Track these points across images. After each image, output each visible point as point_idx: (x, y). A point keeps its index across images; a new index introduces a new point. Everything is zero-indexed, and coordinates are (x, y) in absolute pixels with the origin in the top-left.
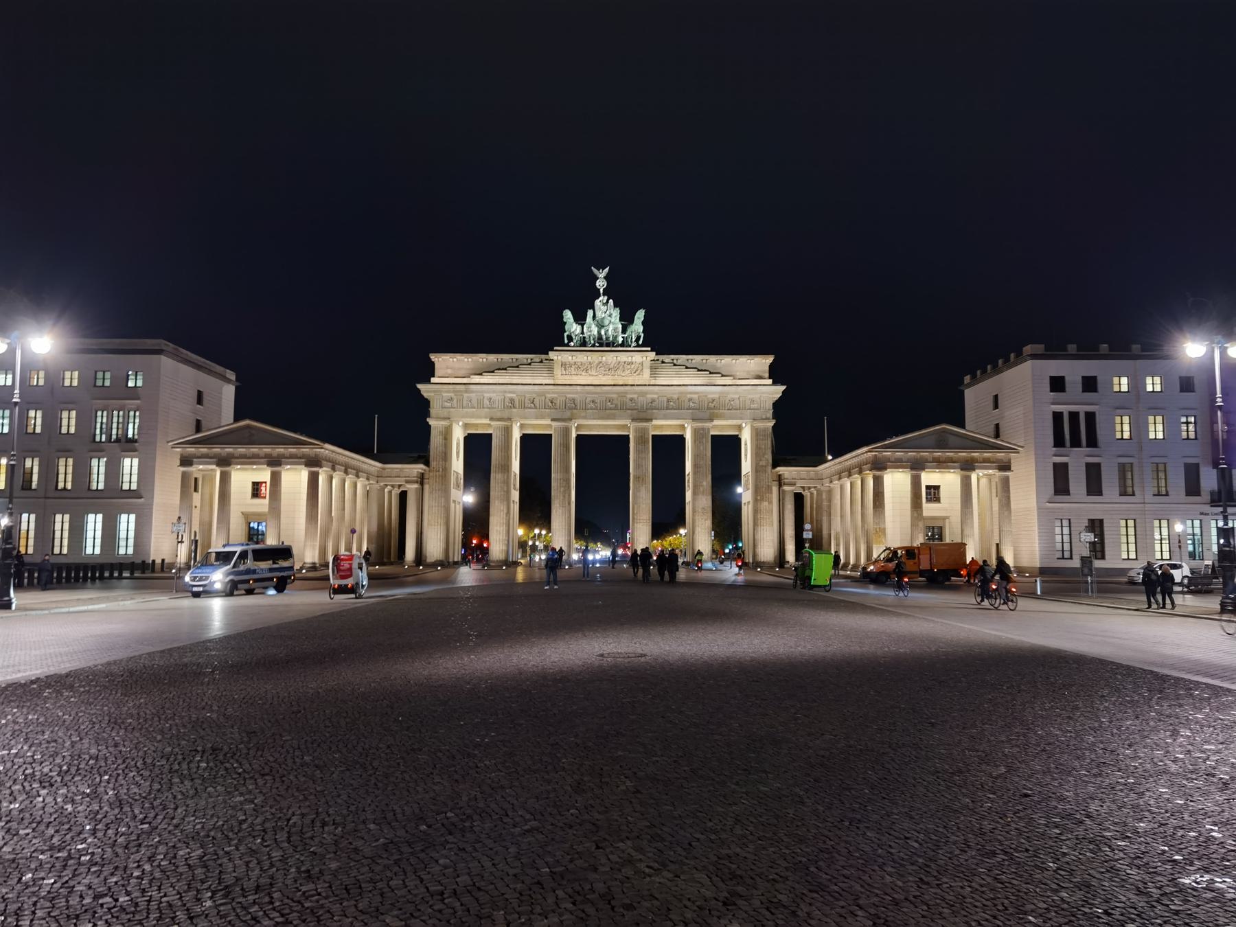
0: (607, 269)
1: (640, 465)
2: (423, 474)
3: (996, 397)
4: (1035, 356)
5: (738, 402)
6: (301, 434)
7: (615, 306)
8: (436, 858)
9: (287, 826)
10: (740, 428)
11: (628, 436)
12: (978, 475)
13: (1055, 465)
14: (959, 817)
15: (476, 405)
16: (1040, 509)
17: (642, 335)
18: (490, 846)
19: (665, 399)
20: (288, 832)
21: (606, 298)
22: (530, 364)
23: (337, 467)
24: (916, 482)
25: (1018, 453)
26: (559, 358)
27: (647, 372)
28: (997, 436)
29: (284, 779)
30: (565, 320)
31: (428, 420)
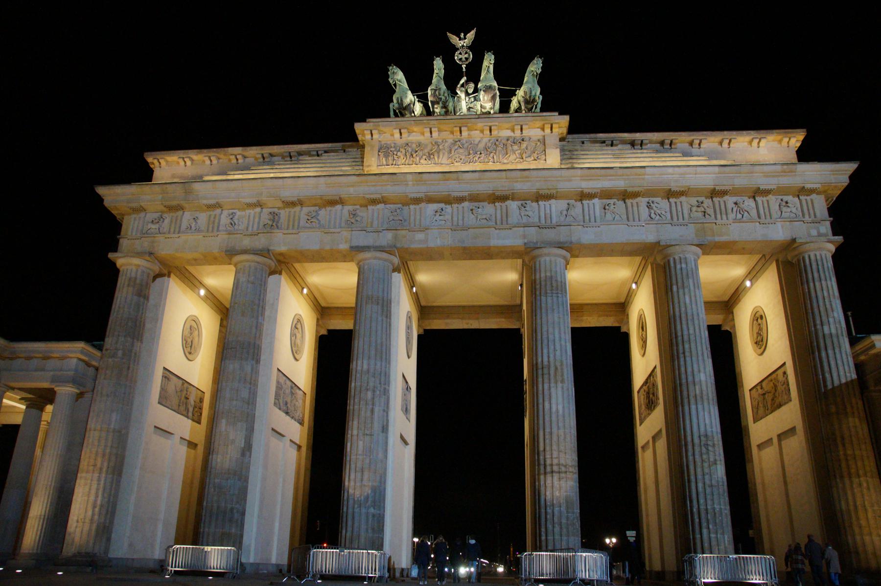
0: (473, 33)
5: (753, 204)
11: (519, 330)
26: (375, 136)
31: (111, 256)
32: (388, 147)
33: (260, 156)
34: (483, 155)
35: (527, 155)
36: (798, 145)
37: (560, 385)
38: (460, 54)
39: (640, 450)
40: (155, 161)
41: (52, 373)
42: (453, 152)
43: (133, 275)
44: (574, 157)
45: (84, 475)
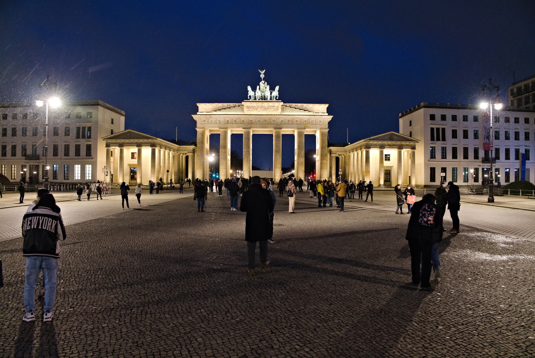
0: (265, 70)
1: (277, 145)
2: (194, 149)
3: (411, 122)
4: (424, 107)
6: (148, 135)
7: (268, 84)
8: (196, 337)
9: (130, 313)
10: (315, 132)
14: (429, 307)
16: (425, 163)
17: (278, 96)
18: (221, 331)
20: (131, 317)
21: (264, 81)
22: (234, 107)
23: (162, 147)
24: (381, 153)
27: (280, 110)
28: (411, 136)
29: (132, 286)
31: (196, 128)
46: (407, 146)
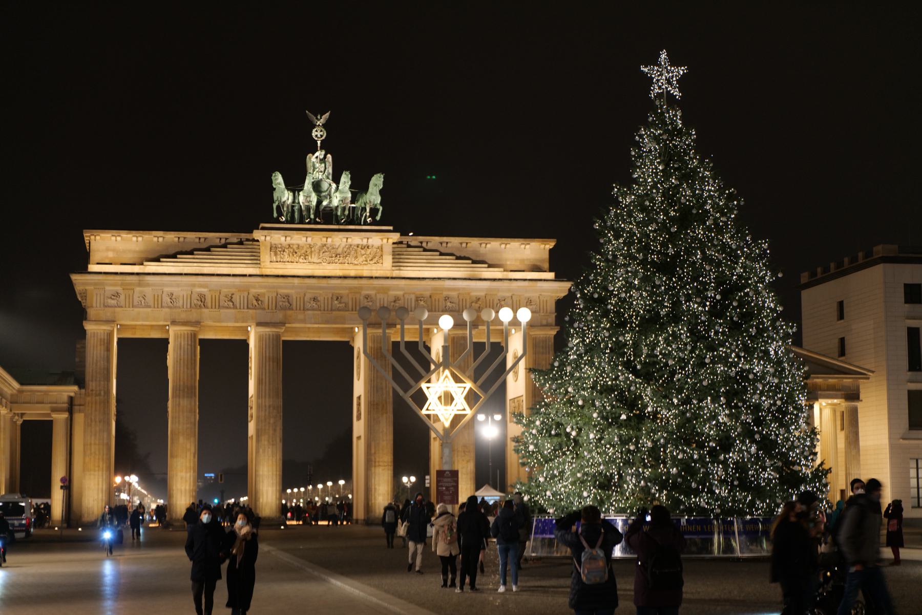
0: (327, 114)
2: (71, 399)
3: (841, 304)
4: (886, 260)
5: (511, 302)
12: (821, 404)
13: (910, 393)
15: (151, 304)
16: (893, 447)
17: (381, 208)
19: (413, 297)
21: (323, 152)
22: (225, 246)
25: (868, 378)
26: (268, 238)
27: (388, 260)
28: (842, 353)
30: (274, 187)
32: (276, 248)
33: (177, 239)
34: (341, 258)
35: (370, 259)
36: (551, 247)
37: (385, 415)
38: (317, 131)
39: (432, 440)
40: (92, 237)
41: (50, 405)
42: (321, 254)
43: (102, 337)
44: (401, 260)
45: (92, 473)
46: (830, 391)
